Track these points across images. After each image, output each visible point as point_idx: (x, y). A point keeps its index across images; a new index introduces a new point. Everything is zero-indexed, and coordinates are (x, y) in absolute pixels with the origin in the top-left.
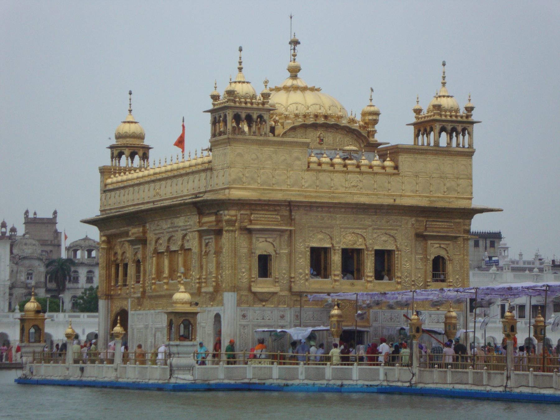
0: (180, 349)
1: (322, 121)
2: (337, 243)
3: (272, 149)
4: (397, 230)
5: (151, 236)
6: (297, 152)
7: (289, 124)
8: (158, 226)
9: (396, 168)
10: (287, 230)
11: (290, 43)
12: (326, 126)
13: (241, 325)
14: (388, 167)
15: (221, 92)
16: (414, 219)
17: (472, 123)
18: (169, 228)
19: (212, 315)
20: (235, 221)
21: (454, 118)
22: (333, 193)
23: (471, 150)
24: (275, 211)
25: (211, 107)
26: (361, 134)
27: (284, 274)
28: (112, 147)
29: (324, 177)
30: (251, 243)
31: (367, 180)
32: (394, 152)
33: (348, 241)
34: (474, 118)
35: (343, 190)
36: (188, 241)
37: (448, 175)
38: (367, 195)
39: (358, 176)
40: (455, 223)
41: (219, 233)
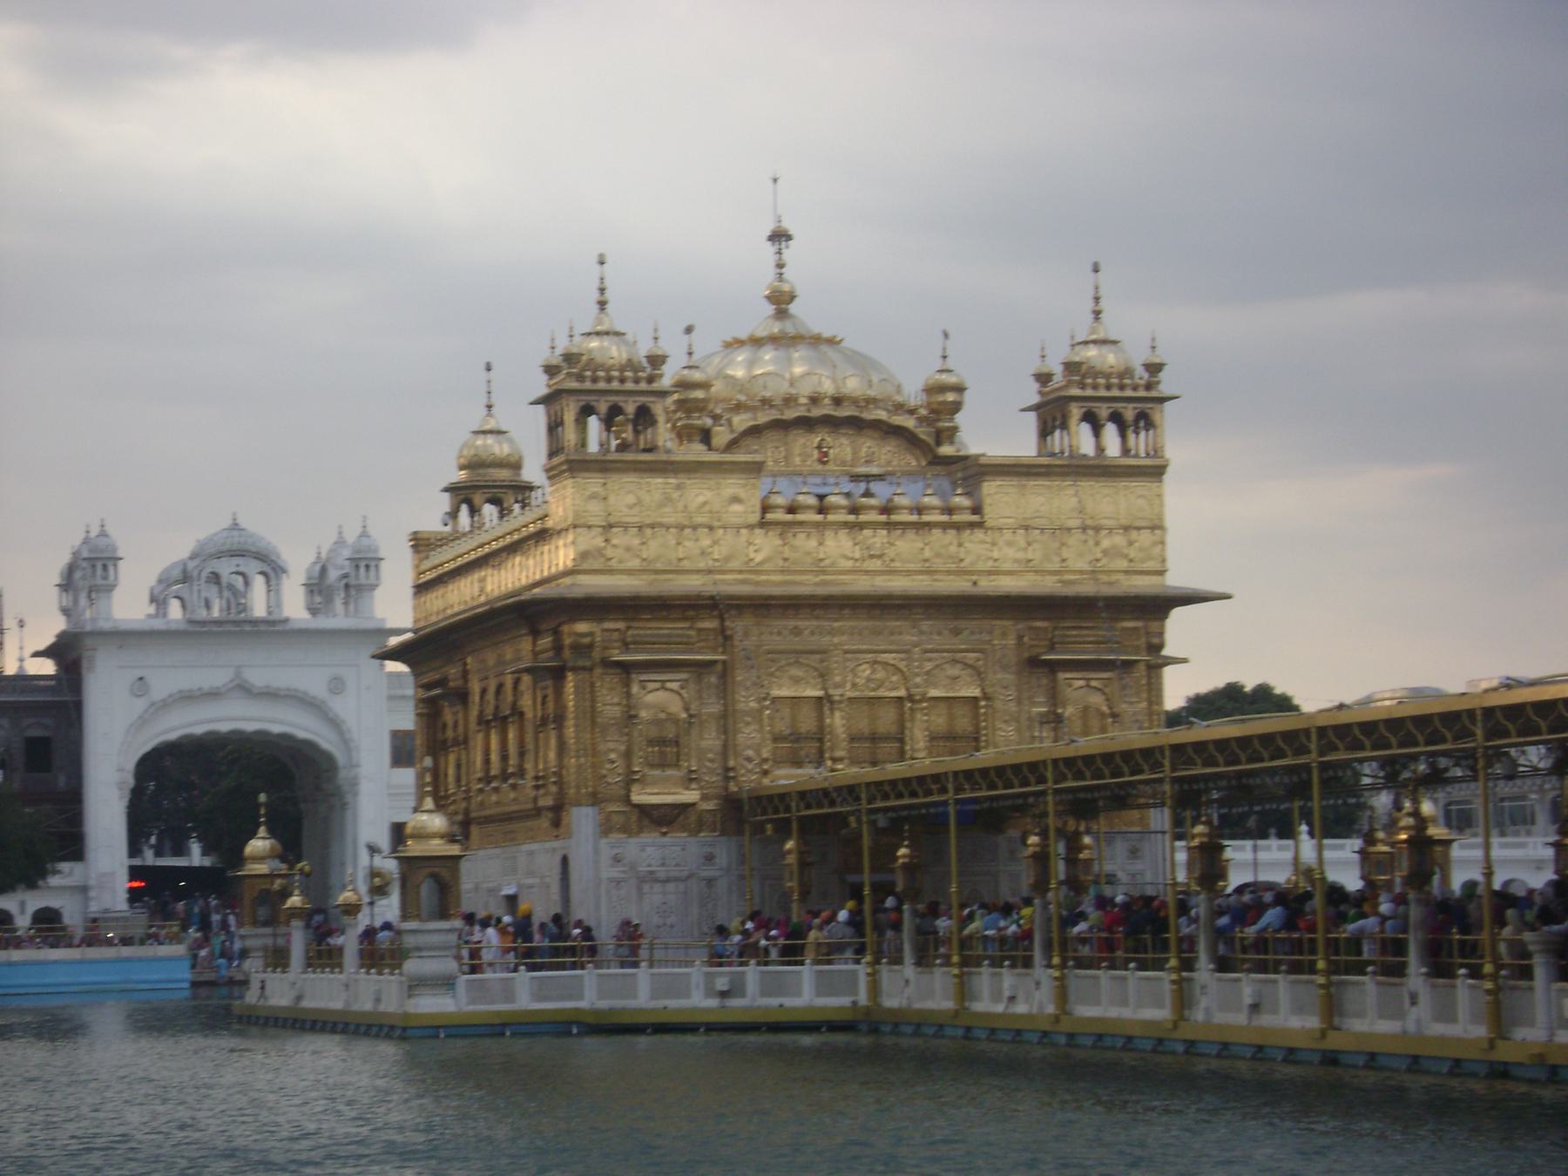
1: (826, 409)
2: (837, 686)
6: (732, 485)
7: (741, 421)
10: (715, 662)
13: (611, 880)
16: (1021, 626)
19: (557, 859)
20: (591, 646)
23: (1157, 462)
24: (685, 619)
26: (923, 434)
27: (711, 761)
28: (451, 489)
31: (907, 546)
32: (971, 473)
34: (1165, 389)
38: (909, 573)
41: (558, 674)
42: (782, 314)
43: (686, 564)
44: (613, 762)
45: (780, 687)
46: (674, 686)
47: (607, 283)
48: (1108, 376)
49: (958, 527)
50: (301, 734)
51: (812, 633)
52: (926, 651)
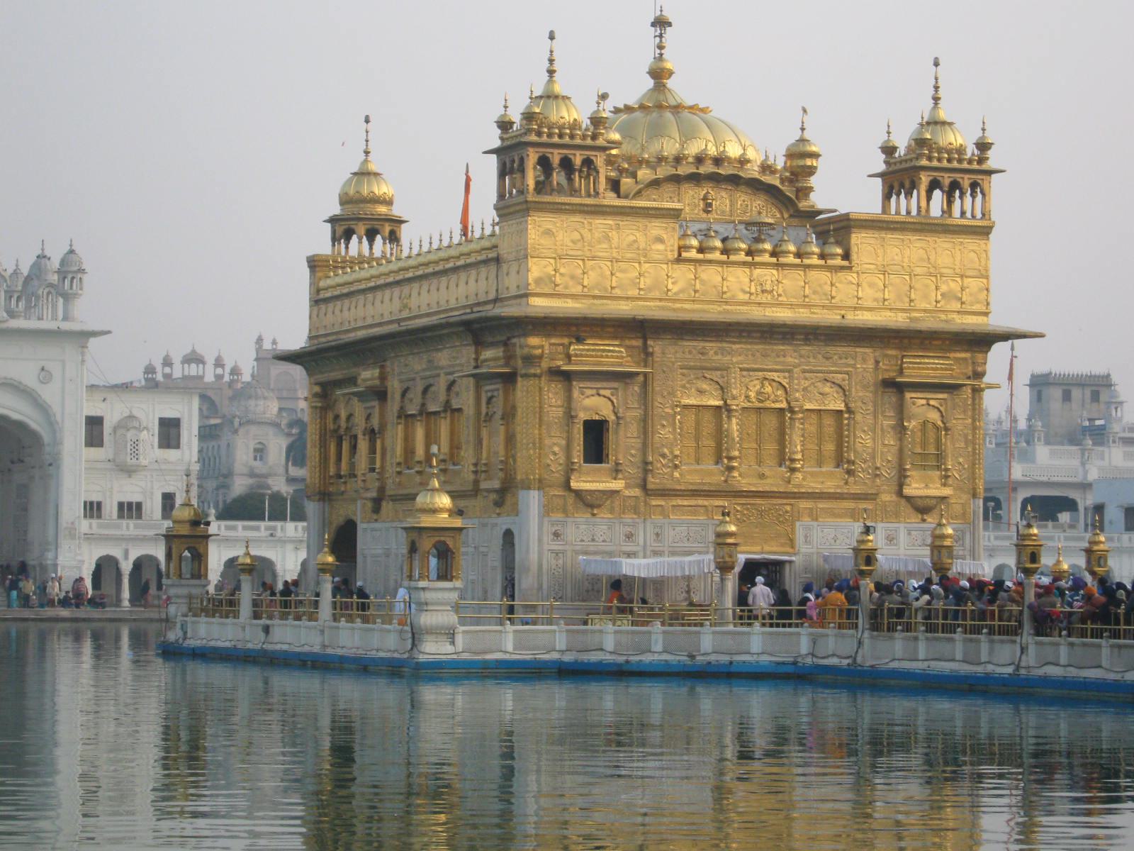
1: (707, 168)
2: (734, 398)
3: (610, 222)
4: (847, 373)
5: (394, 386)
6: (657, 228)
7: (644, 174)
8: (406, 365)
10: (637, 374)
11: (653, 25)
12: (715, 179)
13: (552, 551)
15: (516, 116)
17: (990, 173)
18: (424, 370)
19: (499, 532)
20: (541, 357)
21: (955, 164)
23: (984, 223)
25: (497, 143)
26: (784, 190)
27: (633, 456)
28: (333, 220)
29: (711, 275)
30: (569, 398)
34: (991, 164)
35: (743, 297)
36: (457, 394)
37: (944, 271)
39: (775, 272)
40: (956, 359)
41: (509, 379)
43: (617, 292)
44: (555, 454)
45: (689, 397)
46: (607, 393)
47: (555, 56)
48: (949, 152)
50: (15, 416)
51: (716, 353)
52: (804, 371)
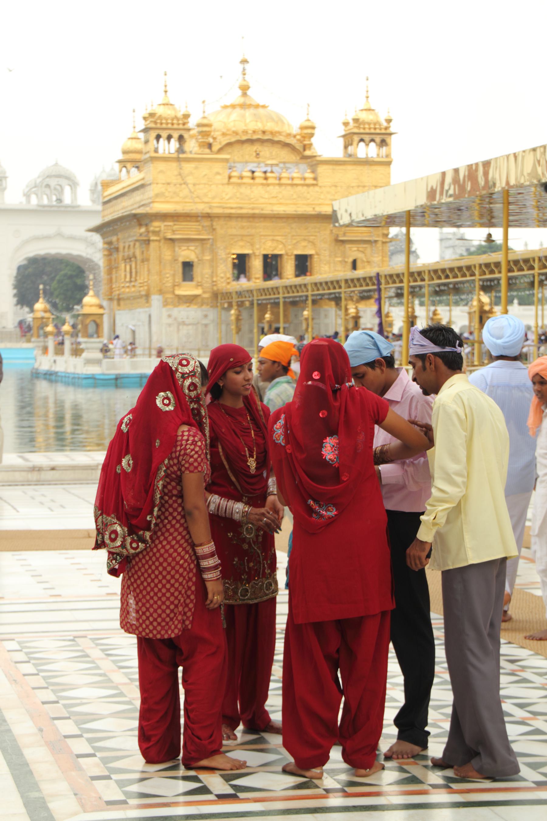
0: (89, 345)
2: (257, 249)
4: (315, 236)
6: (218, 167)
9: (315, 179)
10: (209, 239)
14: (308, 178)
17: (391, 134)
20: (159, 231)
22: (253, 203)
26: (299, 148)
27: (207, 278)
28: (120, 162)
29: (243, 189)
31: (288, 191)
33: (270, 248)
41: (148, 242)
42: (245, 94)
46: (193, 248)
48: (369, 124)
49: (308, 185)
52: (293, 236)
